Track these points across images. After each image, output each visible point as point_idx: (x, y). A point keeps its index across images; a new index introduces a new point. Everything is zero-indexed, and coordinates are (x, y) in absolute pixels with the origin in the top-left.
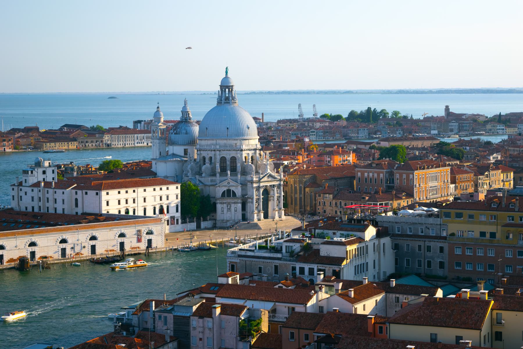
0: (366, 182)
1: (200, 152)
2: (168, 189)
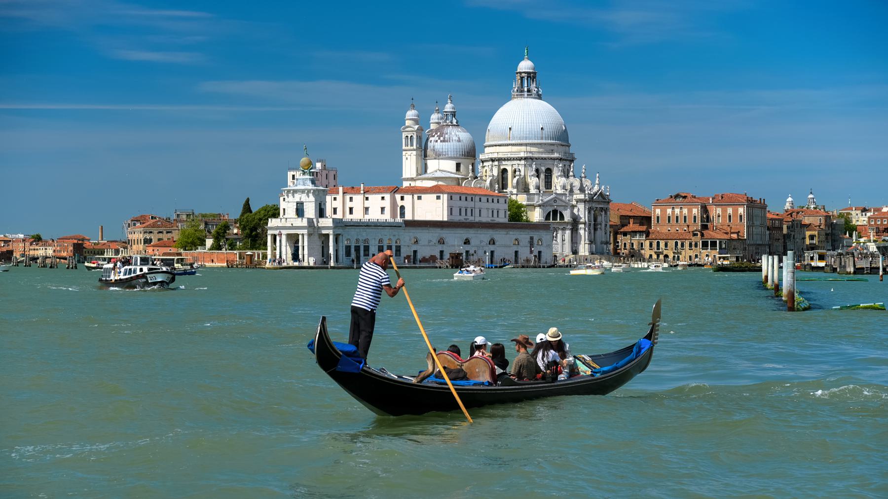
2: (498, 202)
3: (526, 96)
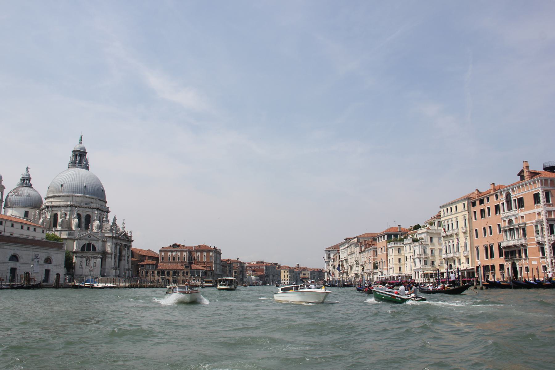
0: (169, 260)
1: (52, 209)
2: (35, 230)
3: (77, 166)
